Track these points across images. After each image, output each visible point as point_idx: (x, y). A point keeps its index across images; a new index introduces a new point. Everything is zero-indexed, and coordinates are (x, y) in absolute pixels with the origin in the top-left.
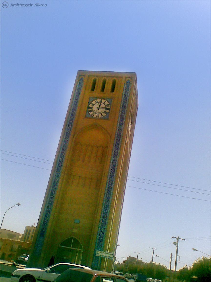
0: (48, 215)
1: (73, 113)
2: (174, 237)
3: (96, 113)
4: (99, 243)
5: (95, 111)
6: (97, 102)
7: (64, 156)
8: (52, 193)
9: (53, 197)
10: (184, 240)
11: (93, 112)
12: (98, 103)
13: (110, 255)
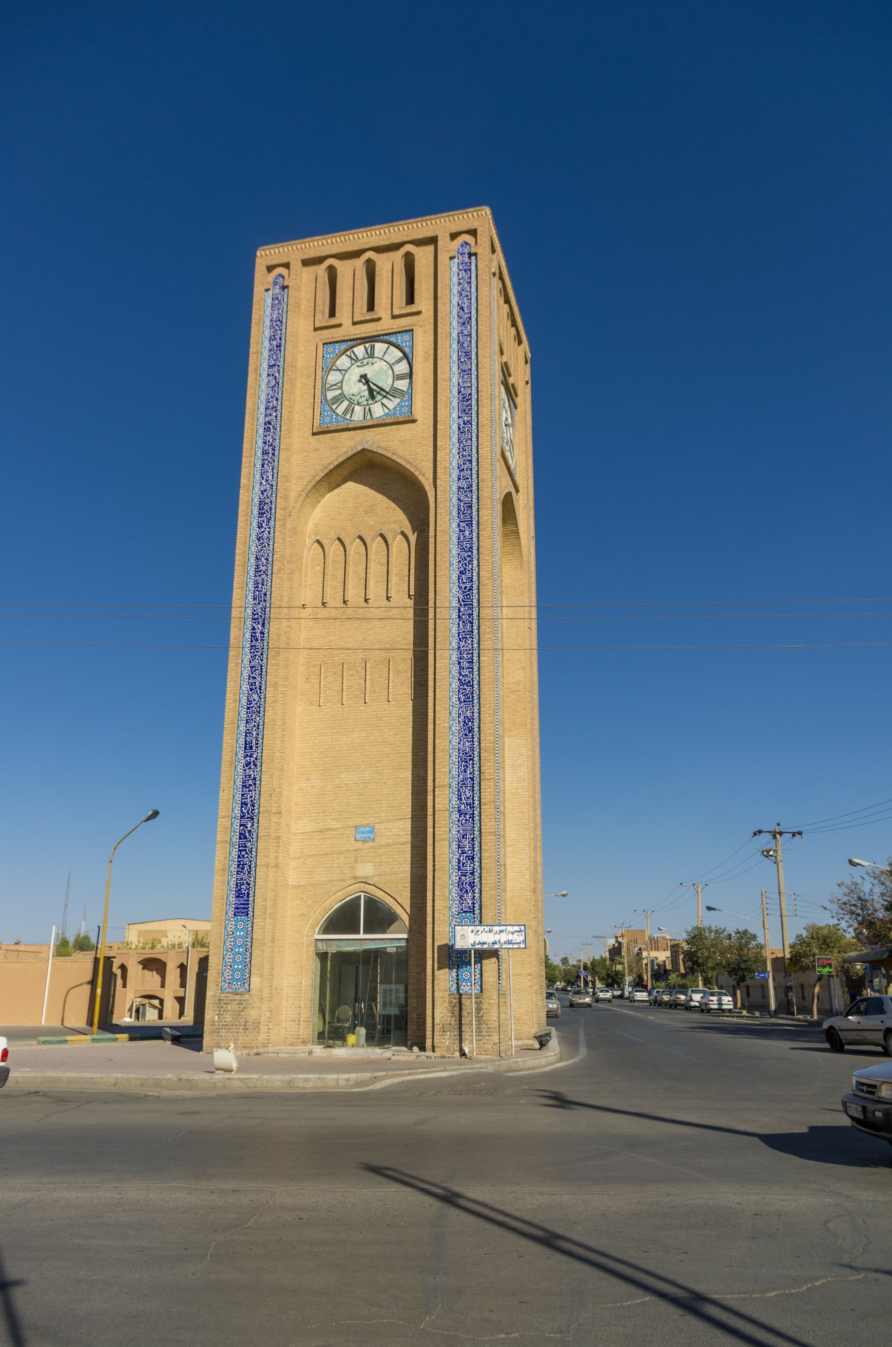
0: (249, 831)
1: (269, 423)
2: (760, 832)
3: (359, 404)
4: (461, 897)
5: (354, 398)
6: (357, 360)
7: (265, 595)
9: (256, 759)
10: (800, 833)
11: (346, 404)
12: (359, 364)
13: (510, 937)
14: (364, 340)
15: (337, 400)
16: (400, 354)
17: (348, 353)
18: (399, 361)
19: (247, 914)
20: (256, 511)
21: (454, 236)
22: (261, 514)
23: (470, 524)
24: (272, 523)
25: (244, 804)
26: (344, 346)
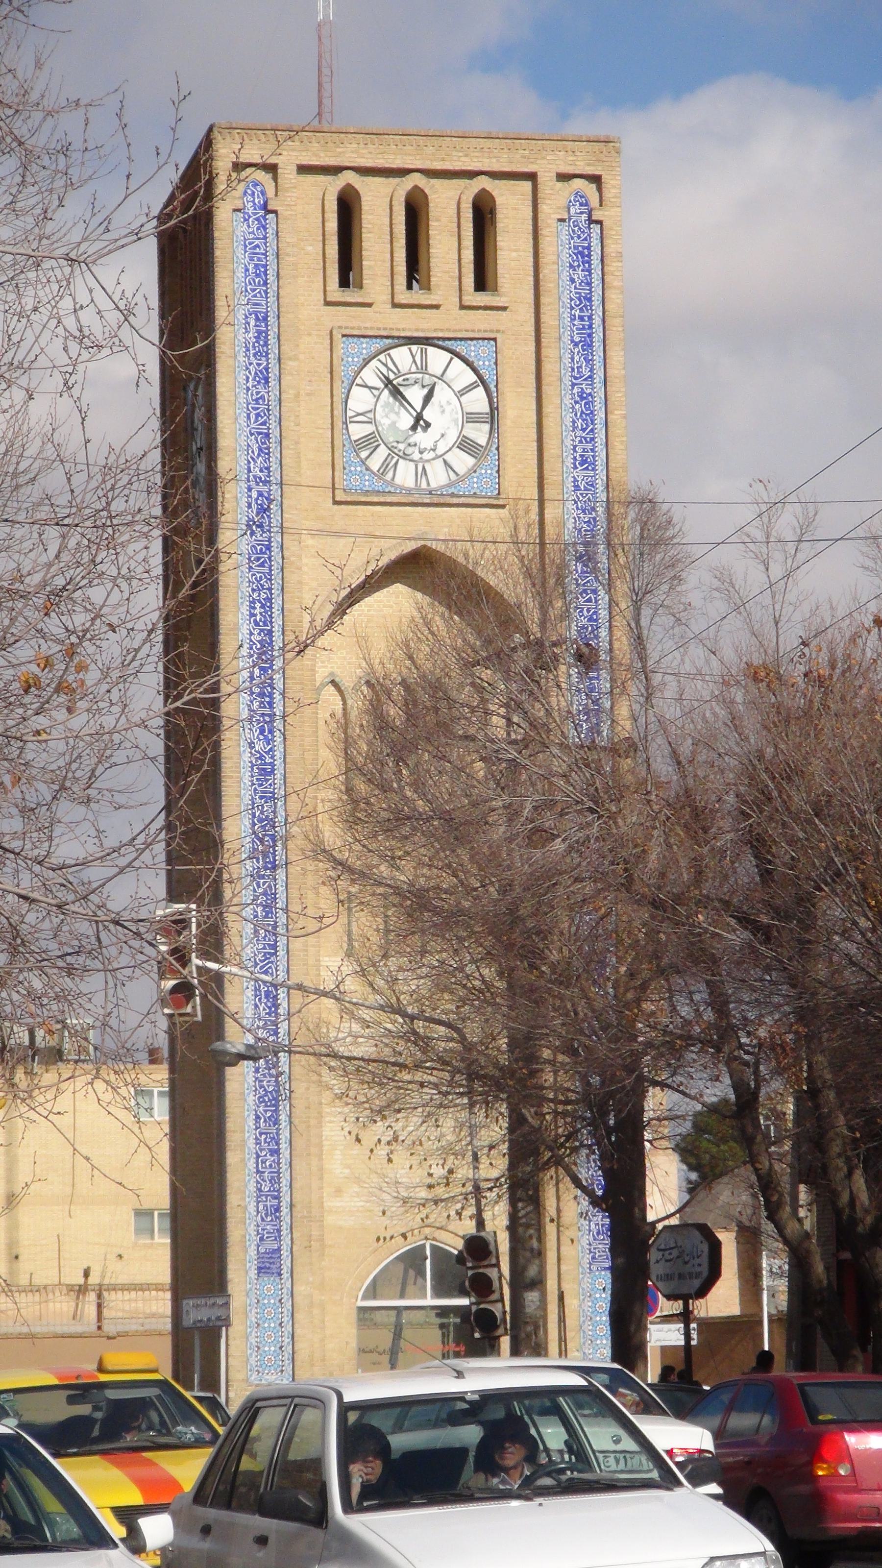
11: (383, 452)
14: (411, 341)
15: (371, 442)
16: (473, 377)
17: (382, 357)
19: (280, 1274)
21: (564, 177)
26: (378, 345)
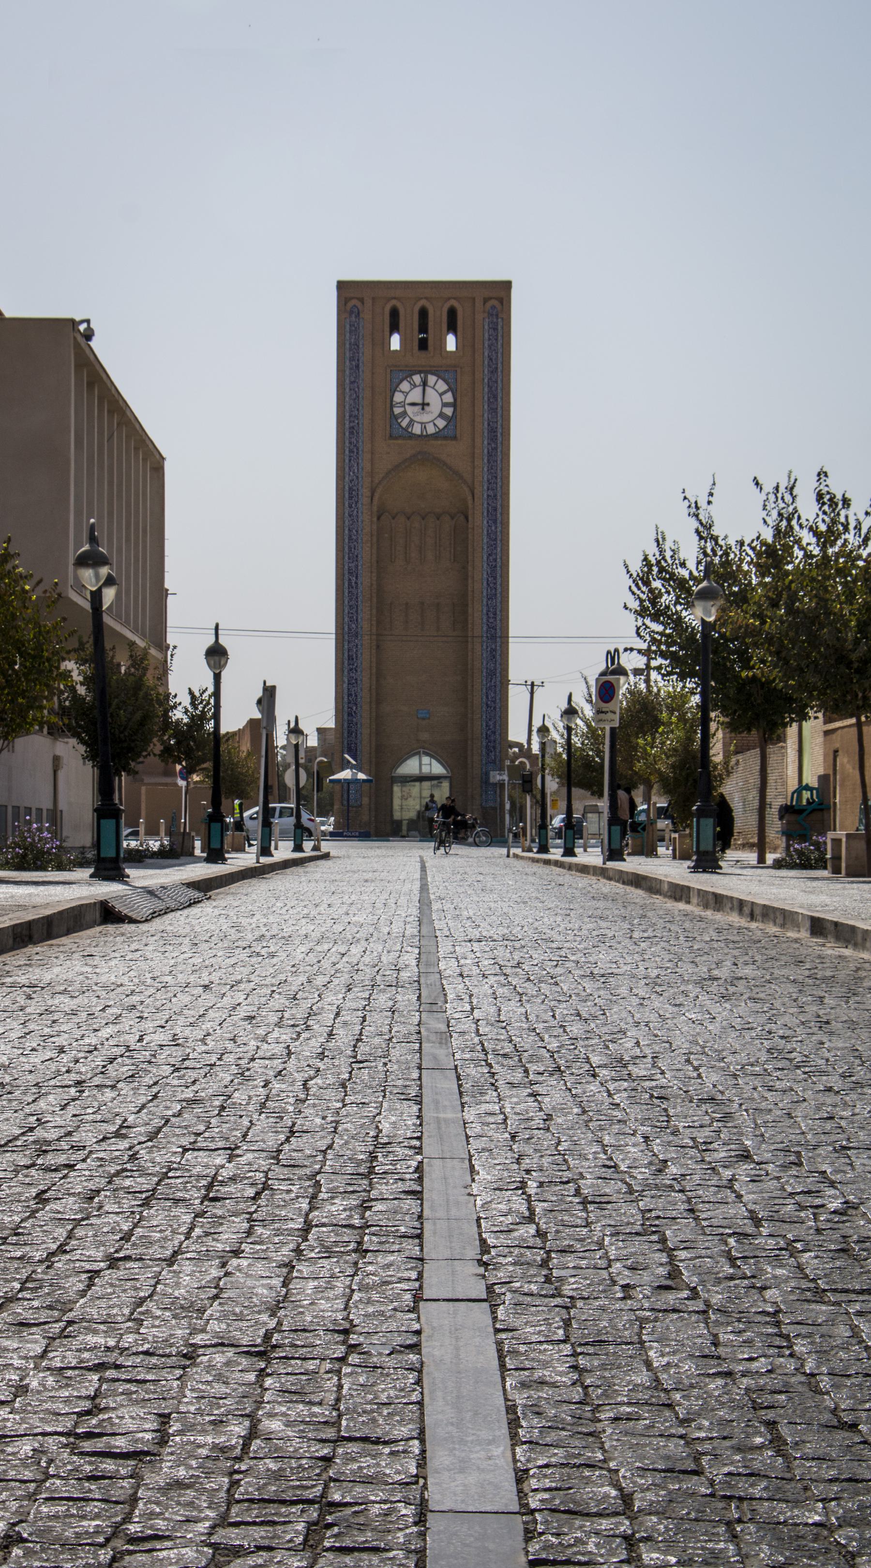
8: (350, 658)
14: (420, 372)
18: (445, 392)
20: (347, 495)
22: (351, 498)
23: (495, 522)
24: (360, 505)
25: (350, 695)
